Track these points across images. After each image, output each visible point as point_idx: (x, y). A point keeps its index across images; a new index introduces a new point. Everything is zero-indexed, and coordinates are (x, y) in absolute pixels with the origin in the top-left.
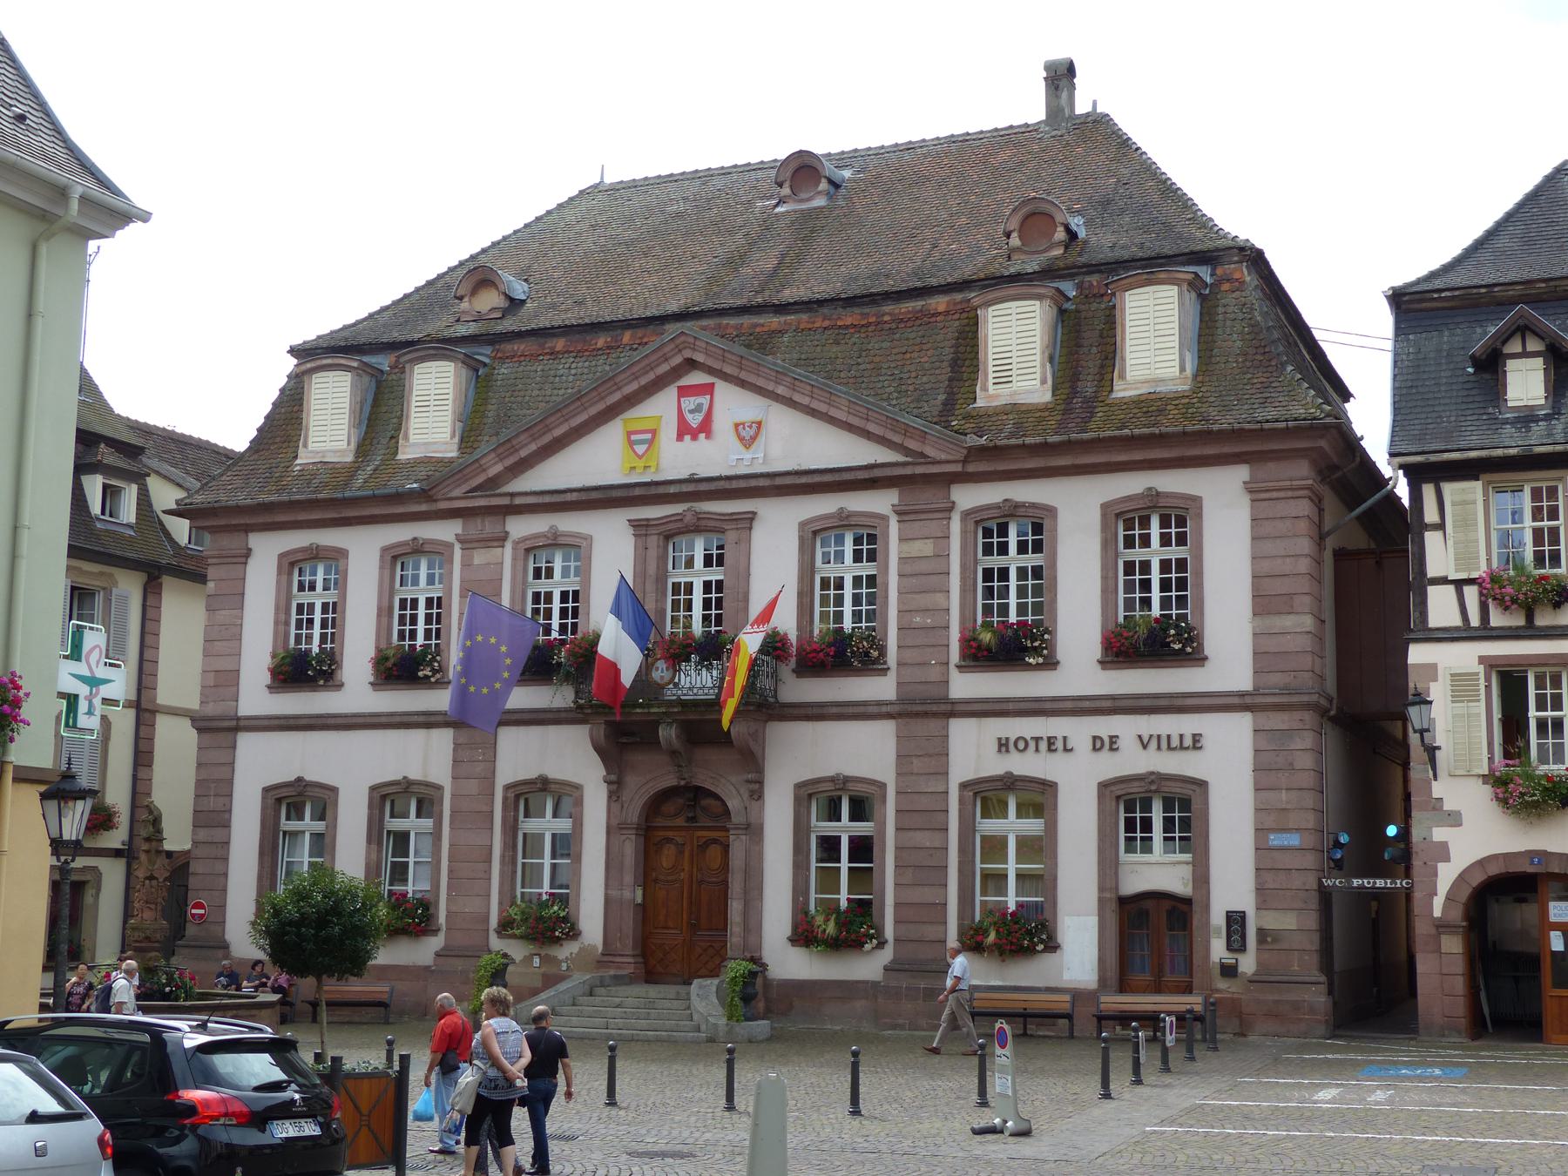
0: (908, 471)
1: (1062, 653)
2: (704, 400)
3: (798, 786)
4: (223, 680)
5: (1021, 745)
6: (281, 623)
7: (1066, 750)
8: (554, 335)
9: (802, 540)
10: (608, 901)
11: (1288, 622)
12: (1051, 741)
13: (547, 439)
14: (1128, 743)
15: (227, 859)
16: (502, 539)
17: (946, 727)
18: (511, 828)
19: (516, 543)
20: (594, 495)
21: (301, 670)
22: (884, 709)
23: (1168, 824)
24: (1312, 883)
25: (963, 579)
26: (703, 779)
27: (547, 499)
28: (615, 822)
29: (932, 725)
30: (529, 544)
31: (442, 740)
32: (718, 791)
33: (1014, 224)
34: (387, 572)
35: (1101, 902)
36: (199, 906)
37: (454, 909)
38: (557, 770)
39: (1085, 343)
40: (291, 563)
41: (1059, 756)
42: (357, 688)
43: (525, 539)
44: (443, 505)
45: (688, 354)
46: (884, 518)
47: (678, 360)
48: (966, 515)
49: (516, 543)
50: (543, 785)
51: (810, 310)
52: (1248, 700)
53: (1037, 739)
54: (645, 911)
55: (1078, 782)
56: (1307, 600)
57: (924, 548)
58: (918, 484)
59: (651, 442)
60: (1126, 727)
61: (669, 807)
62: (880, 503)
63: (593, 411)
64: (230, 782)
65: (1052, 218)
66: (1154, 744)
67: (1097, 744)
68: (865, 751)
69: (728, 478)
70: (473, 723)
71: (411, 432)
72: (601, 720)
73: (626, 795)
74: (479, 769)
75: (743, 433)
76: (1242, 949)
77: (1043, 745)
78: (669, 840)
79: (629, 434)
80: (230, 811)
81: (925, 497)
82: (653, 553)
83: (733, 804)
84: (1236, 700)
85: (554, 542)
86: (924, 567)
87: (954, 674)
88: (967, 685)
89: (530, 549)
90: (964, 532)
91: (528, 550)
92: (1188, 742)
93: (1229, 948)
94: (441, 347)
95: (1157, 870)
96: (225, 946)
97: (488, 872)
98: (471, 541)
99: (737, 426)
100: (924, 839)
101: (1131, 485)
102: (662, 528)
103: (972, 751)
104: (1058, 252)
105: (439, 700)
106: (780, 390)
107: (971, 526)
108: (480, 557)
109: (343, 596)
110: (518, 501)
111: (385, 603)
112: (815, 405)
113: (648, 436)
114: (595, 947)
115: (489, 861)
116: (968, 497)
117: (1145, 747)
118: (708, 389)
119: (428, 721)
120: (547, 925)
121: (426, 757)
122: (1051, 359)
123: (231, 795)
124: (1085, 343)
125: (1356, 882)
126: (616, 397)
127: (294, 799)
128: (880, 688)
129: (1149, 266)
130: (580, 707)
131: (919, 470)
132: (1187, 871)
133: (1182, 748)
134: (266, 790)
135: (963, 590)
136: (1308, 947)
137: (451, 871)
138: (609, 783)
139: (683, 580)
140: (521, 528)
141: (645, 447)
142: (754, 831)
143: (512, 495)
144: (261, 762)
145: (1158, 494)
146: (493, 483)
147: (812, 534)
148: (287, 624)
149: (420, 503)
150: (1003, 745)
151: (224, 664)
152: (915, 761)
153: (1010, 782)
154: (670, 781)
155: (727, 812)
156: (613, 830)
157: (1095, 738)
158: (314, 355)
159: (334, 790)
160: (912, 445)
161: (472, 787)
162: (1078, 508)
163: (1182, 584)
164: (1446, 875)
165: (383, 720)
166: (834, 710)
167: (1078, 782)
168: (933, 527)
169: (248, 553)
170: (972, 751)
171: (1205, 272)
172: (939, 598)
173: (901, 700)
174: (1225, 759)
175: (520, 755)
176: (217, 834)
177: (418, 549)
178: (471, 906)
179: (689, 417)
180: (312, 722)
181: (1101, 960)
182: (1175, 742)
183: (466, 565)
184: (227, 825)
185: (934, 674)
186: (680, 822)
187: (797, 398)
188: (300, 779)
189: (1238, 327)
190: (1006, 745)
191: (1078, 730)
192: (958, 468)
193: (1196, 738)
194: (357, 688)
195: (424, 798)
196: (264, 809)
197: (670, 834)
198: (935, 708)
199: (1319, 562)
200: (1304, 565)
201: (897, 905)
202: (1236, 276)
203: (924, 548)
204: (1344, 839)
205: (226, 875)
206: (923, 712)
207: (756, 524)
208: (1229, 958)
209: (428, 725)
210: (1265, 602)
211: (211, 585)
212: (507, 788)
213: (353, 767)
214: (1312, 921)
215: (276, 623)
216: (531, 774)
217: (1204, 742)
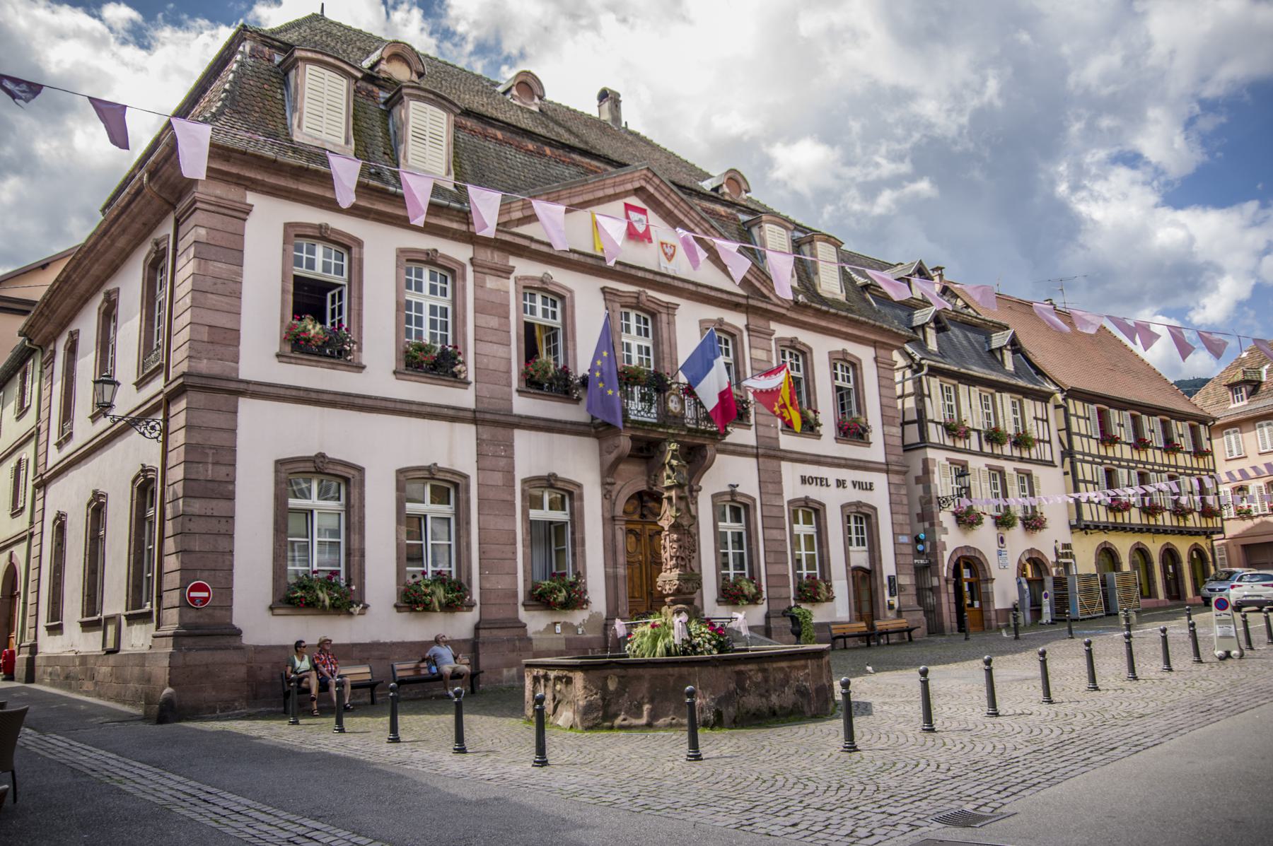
4: (226, 339)
15: (232, 536)
16: (507, 272)
30: (528, 283)
37: (488, 586)
42: (378, 371)
43: (526, 278)
45: (643, 183)
47: (637, 185)
50: (550, 481)
62: (737, 320)
64: (233, 450)
70: (493, 423)
74: (502, 463)
75: (667, 250)
80: (233, 482)
89: (530, 289)
97: (514, 553)
100: (775, 534)
105: (465, 398)
108: (491, 282)
114: (600, 614)
115: (514, 544)
116: (782, 331)
119: (453, 415)
121: (456, 449)
132: (866, 555)
144: (265, 436)
149: (451, 220)
150: (804, 480)
156: (610, 520)
159: (361, 470)
161: (497, 478)
164: (947, 555)
165: (414, 408)
166: (732, 448)
169: (247, 210)
175: (532, 455)
176: (218, 507)
177: (430, 259)
179: (636, 225)
180: (338, 398)
183: (479, 285)
184: (231, 497)
191: (831, 474)
194: (378, 371)
195: (446, 486)
212: (525, 481)
213: (384, 450)
217: (874, 486)
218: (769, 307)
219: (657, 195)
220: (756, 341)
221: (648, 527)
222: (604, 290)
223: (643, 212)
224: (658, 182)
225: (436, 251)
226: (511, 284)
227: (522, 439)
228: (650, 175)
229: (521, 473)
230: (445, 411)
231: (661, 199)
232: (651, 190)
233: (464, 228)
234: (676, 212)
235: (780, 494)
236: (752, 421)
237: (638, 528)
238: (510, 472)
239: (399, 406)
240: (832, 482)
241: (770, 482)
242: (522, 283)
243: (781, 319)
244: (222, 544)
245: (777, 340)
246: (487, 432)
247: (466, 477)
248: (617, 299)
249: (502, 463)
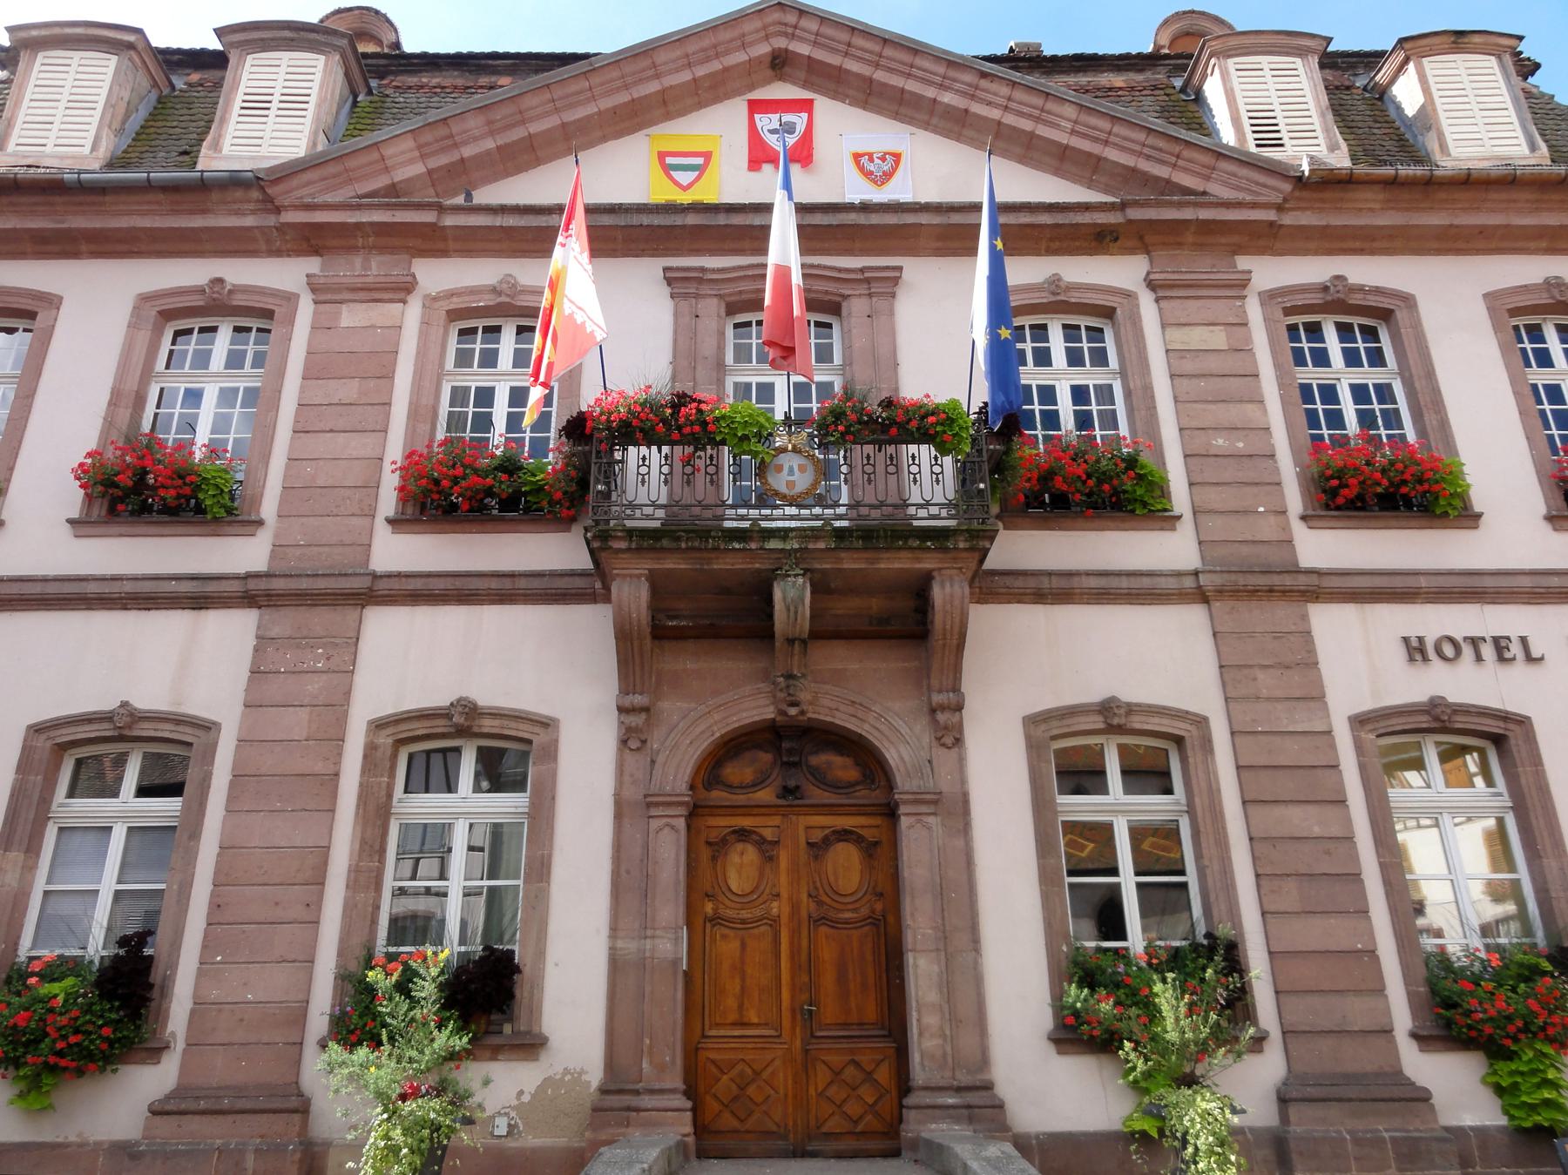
1: (1477, 507)
2: (800, 120)
5: (1450, 649)
7: (1530, 659)
8: (495, 71)
10: (616, 965)
16: (403, 289)
17: (1305, 617)
18: (375, 812)
28: (633, 793)
29: (1280, 614)
30: (457, 303)
31: (230, 636)
32: (864, 730)
38: (499, 688)
41: (1519, 670)
43: (451, 294)
45: (781, 43)
47: (763, 49)
53: (1475, 642)
54: (697, 986)
59: (701, 170)
63: (606, 103)
68: (1159, 659)
74: (314, 686)
75: (870, 167)
77: (1488, 651)
79: (662, 156)
86: (1213, 364)
88: (1328, 548)
97: (314, 906)
98: (338, 288)
99: (857, 157)
102: (728, 289)
103: (1359, 661)
105: (241, 555)
108: (352, 316)
111: (132, 384)
113: (700, 161)
114: (577, 1076)
116: (1271, 273)
118: (806, 106)
119: (200, 595)
121: (192, 667)
137: (216, 906)
139: (754, 380)
141: (692, 175)
142: (955, 809)
149: (238, 213)
150: (1416, 650)
152: (1260, 675)
154: (755, 708)
156: (630, 810)
166: (1093, 582)
168: (1220, 309)
170: (1359, 661)
175: (408, 662)
178: (263, 986)
185: (1267, 529)
186: (766, 795)
190: (1422, 650)
197: (746, 822)
207: (901, 292)
209: (199, 602)
212: (378, 725)
216: (439, 698)
219: (820, 55)
220: (1176, 309)
221: (805, 821)
222: (673, 279)
223: (806, 106)
224: (813, 26)
225: (220, 281)
226: (412, 314)
227: (385, 630)
228: (791, 18)
230: (173, 586)
231: (834, 60)
232: (804, 49)
233: (271, 221)
234: (880, 75)
235: (1315, 697)
237: (767, 827)
238: (337, 707)
239: (52, 589)
241: (1273, 672)
243: (1269, 239)
245: (1268, 297)
246: (285, 621)
248: (706, 289)
249: (314, 686)
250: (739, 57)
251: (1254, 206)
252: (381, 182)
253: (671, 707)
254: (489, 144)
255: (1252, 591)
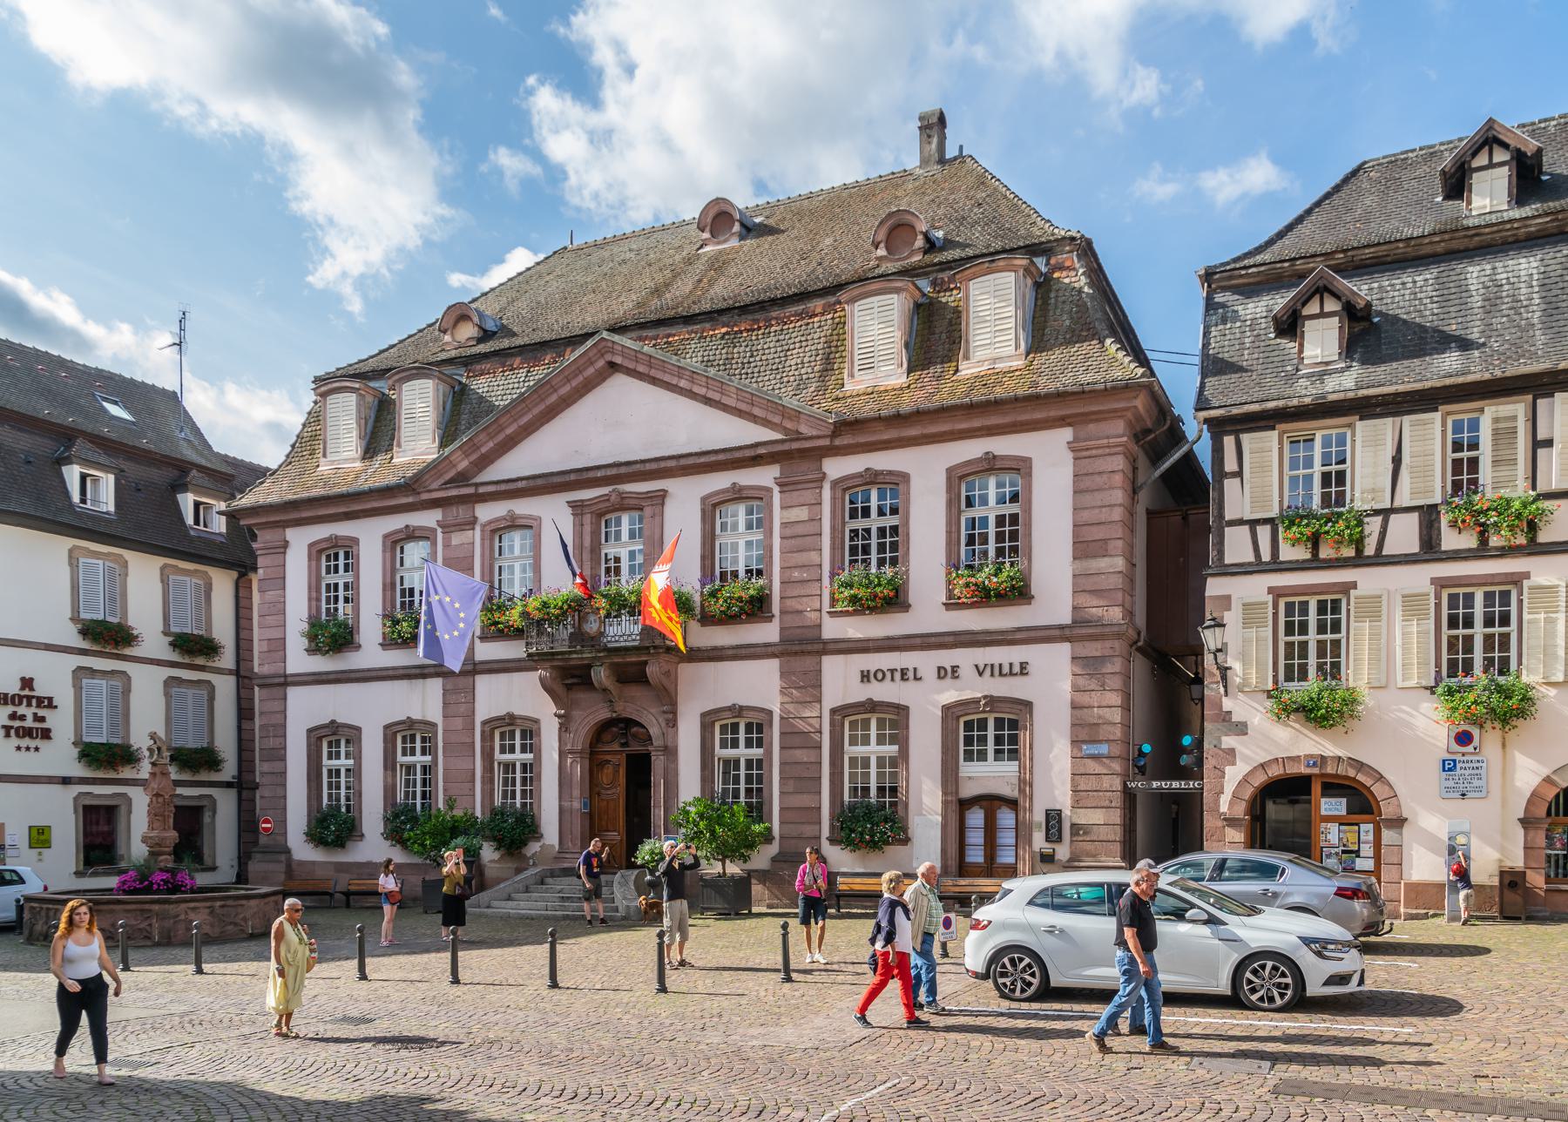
0: (786, 447)
1: (912, 599)
3: (703, 715)
5: (879, 676)
6: (314, 598)
7: (916, 679)
8: (512, 355)
9: (703, 511)
11: (1102, 564)
12: (904, 672)
13: (501, 437)
14: (967, 671)
15: (285, 785)
16: (472, 523)
19: (483, 526)
20: (540, 482)
21: (333, 636)
22: (770, 649)
23: (999, 740)
24: (1117, 783)
25: (833, 538)
26: (629, 711)
27: (503, 487)
29: (808, 662)
30: (493, 526)
33: (882, 236)
34: (388, 555)
35: (945, 803)
36: (267, 821)
39: (935, 335)
40: (318, 551)
41: (911, 684)
43: (490, 522)
44: (425, 496)
45: (609, 357)
46: (769, 490)
47: (601, 363)
48: (835, 484)
49: (483, 526)
51: (712, 319)
52: (1067, 632)
53: (892, 671)
55: (927, 702)
56: (1120, 543)
57: (801, 514)
58: (796, 457)
60: (965, 658)
61: (607, 737)
62: (764, 476)
63: (536, 411)
65: (913, 227)
66: (988, 670)
67: (941, 673)
68: (758, 685)
69: (643, 462)
71: (403, 440)
72: (548, 665)
73: (573, 727)
74: (463, 709)
76: (1060, 839)
77: (898, 675)
78: (608, 762)
80: (285, 748)
81: (803, 469)
82: (587, 529)
83: (654, 731)
84: (1057, 632)
85: (513, 524)
86: (800, 530)
87: (826, 619)
90: (833, 499)
91: (494, 531)
92: (1017, 669)
93: (1048, 839)
94: (421, 370)
95: (989, 774)
96: (288, 851)
101: (972, 450)
102: (594, 508)
103: (841, 681)
104: (917, 258)
106: (683, 383)
107: (839, 494)
108: (457, 539)
109: (357, 577)
110: (481, 490)
112: (710, 394)
115: (473, 781)
116: (836, 468)
117: (981, 674)
120: (514, 831)
121: (424, 701)
122: (907, 345)
123: (285, 736)
124: (935, 335)
125: (1155, 784)
126: (553, 398)
127: (333, 736)
128: (767, 632)
129: (989, 259)
130: (529, 655)
131: (795, 445)
133: (1011, 674)
134: (310, 731)
135: (833, 548)
136: (1112, 837)
138: (559, 716)
140: (487, 512)
142: (671, 752)
143: (477, 485)
144: (305, 709)
145: (995, 457)
146: (462, 479)
147: (711, 508)
148: (318, 600)
150: (865, 677)
151: (276, 634)
153: (871, 706)
154: (604, 714)
155: (650, 738)
157: (939, 668)
158: (326, 385)
159: (359, 729)
160: (789, 425)
161: (458, 723)
162: (926, 470)
163: (1014, 536)
167: (927, 702)
168: (808, 496)
170: (841, 681)
171: (1040, 262)
172: (813, 556)
173: (783, 641)
174: (1050, 681)
176: (277, 766)
177: (411, 535)
181: (944, 851)
182: (1006, 670)
183: (446, 545)
184: (283, 759)
186: (616, 747)
187: (696, 389)
188: (333, 722)
189: (1067, 308)
191: (926, 661)
192: (827, 442)
193: (1023, 666)
196: (309, 745)
198: (809, 647)
199: (1131, 514)
200: (1117, 514)
201: (782, 809)
202: (1068, 264)
203: (801, 514)
204: (1147, 748)
205: (285, 797)
206: (803, 650)
207: (668, 502)
208: (1047, 847)
209: (424, 676)
210: (1084, 548)
211: (260, 571)
212: (484, 723)
213: (371, 709)
214: (1116, 816)
215: (310, 599)
216: (500, 711)
218: (807, 444)
227: (483, 683)
229: (482, 713)
236: (776, 609)
240: (928, 672)
242: (488, 528)
244: (279, 792)
247: (434, 725)
248: (586, 510)
250: (591, 371)
251: (818, 437)
252: (452, 474)
253: (576, 713)
254: (491, 444)
255: (803, 650)
